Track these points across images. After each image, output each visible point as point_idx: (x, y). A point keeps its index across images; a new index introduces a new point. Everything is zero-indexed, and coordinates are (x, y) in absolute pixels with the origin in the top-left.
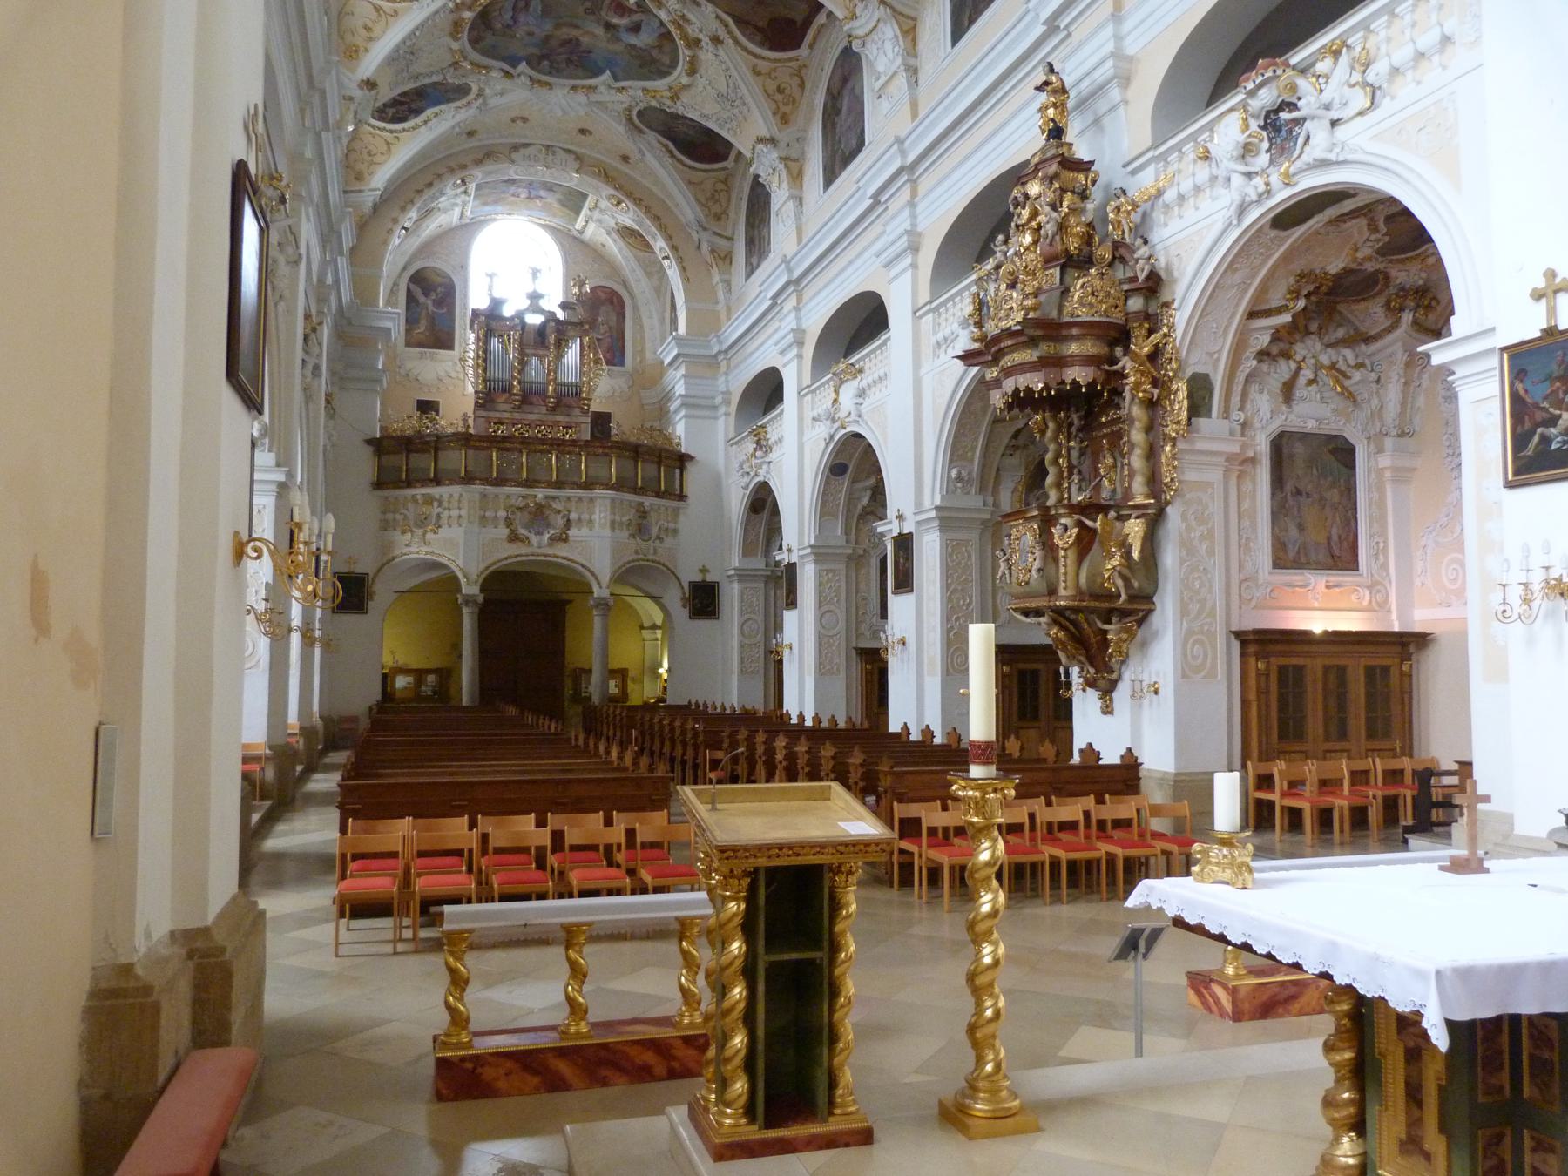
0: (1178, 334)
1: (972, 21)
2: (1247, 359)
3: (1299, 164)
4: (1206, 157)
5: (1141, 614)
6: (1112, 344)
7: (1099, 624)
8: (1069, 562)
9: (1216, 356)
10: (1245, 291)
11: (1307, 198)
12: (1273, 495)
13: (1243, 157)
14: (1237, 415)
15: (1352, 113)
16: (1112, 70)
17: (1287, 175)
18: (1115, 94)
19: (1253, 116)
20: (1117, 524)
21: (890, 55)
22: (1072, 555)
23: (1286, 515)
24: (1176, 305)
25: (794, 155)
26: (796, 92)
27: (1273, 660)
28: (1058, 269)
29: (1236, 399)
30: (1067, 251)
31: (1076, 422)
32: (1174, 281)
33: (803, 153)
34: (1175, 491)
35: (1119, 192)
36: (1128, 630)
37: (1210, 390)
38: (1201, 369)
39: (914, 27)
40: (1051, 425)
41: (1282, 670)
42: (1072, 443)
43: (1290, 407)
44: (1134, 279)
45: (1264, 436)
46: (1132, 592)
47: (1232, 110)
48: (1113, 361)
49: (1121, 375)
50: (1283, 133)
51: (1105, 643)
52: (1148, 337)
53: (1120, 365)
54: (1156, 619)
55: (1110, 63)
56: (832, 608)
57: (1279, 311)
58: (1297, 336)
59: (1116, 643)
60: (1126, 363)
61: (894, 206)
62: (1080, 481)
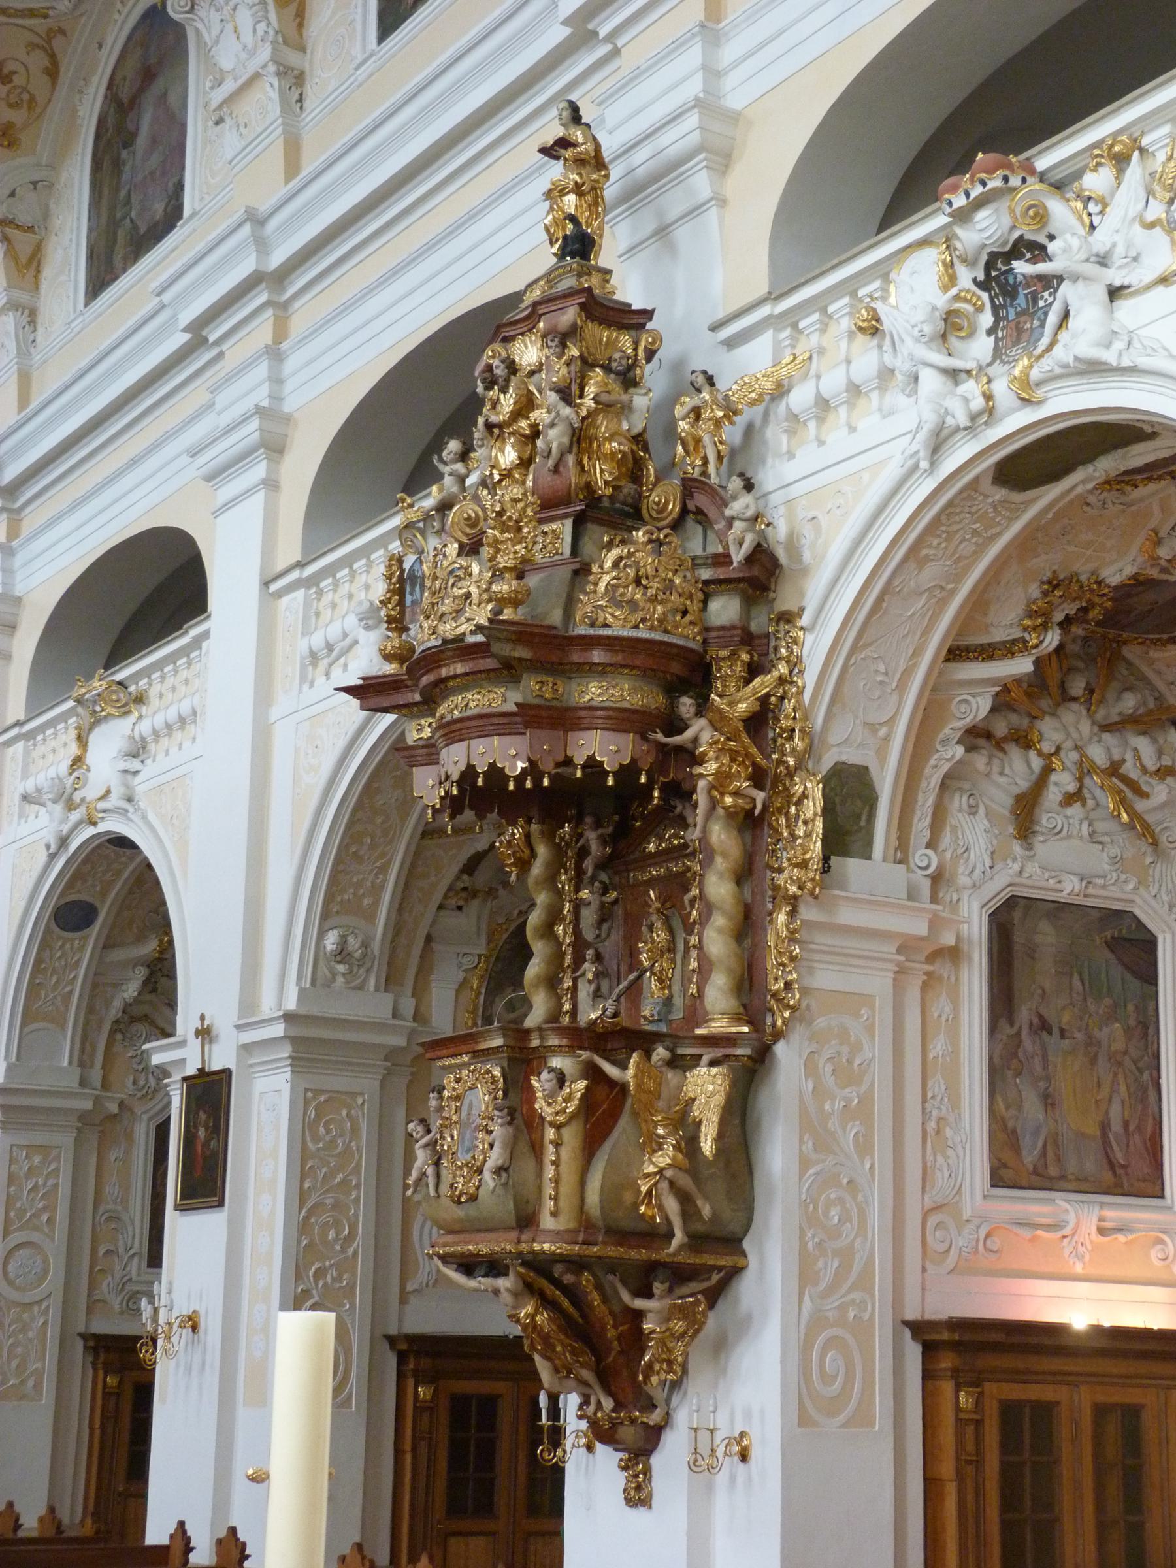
0: (809, 679)
2: (945, 742)
3: (1047, 364)
4: (873, 328)
5: (715, 1277)
6: (673, 690)
7: (626, 1297)
8: (565, 1153)
9: (883, 732)
10: (943, 603)
12: (993, 1028)
13: (944, 337)
14: (921, 856)
15: (1150, 276)
16: (695, 137)
17: (1025, 382)
18: (701, 183)
19: (964, 260)
20: (671, 1076)
21: (248, 38)
23: (1018, 1074)
24: (804, 621)
25: (24, 218)
26: (39, 85)
27: (989, 1387)
28: (569, 524)
29: (921, 825)
30: (589, 488)
31: (594, 847)
32: (804, 571)
33: (46, 215)
34: (794, 1009)
35: (701, 380)
36: (686, 1313)
37: (870, 800)
38: (852, 756)
40: (542, 850)
41: (1010, 1412)
42: (585, 894)
43: (1030, 847)
44: (723, 559)
45: (976, 906)
46: (699, 1227)
47: (924, 242)
48: (675, 725)
49: (690, 756)
50: (1021, 300)
51: (636, 1340)
52: (748, 681)
53: (689, 734)
54: (746, 1288)
56: (35, 1237)
57: (1009, 649)
58: (1045, 703)
59: (662, 1342)
60: (700, 732)
61: (237, 352)
62: (597, 975)
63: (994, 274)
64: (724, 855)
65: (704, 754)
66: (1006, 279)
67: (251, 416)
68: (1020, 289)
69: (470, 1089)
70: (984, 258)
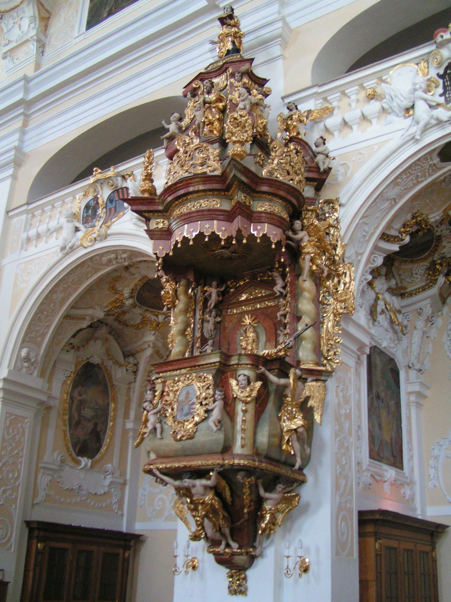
1: (110, 13)
9: (359, 258)
16: (280, 30)
18: (276, 50)
22: (251, 408)
31: (214, 297)
39: (49, 18)
40: (182, 297)
55: (280, 24)
64: (309, 292)
67: (12, 149)
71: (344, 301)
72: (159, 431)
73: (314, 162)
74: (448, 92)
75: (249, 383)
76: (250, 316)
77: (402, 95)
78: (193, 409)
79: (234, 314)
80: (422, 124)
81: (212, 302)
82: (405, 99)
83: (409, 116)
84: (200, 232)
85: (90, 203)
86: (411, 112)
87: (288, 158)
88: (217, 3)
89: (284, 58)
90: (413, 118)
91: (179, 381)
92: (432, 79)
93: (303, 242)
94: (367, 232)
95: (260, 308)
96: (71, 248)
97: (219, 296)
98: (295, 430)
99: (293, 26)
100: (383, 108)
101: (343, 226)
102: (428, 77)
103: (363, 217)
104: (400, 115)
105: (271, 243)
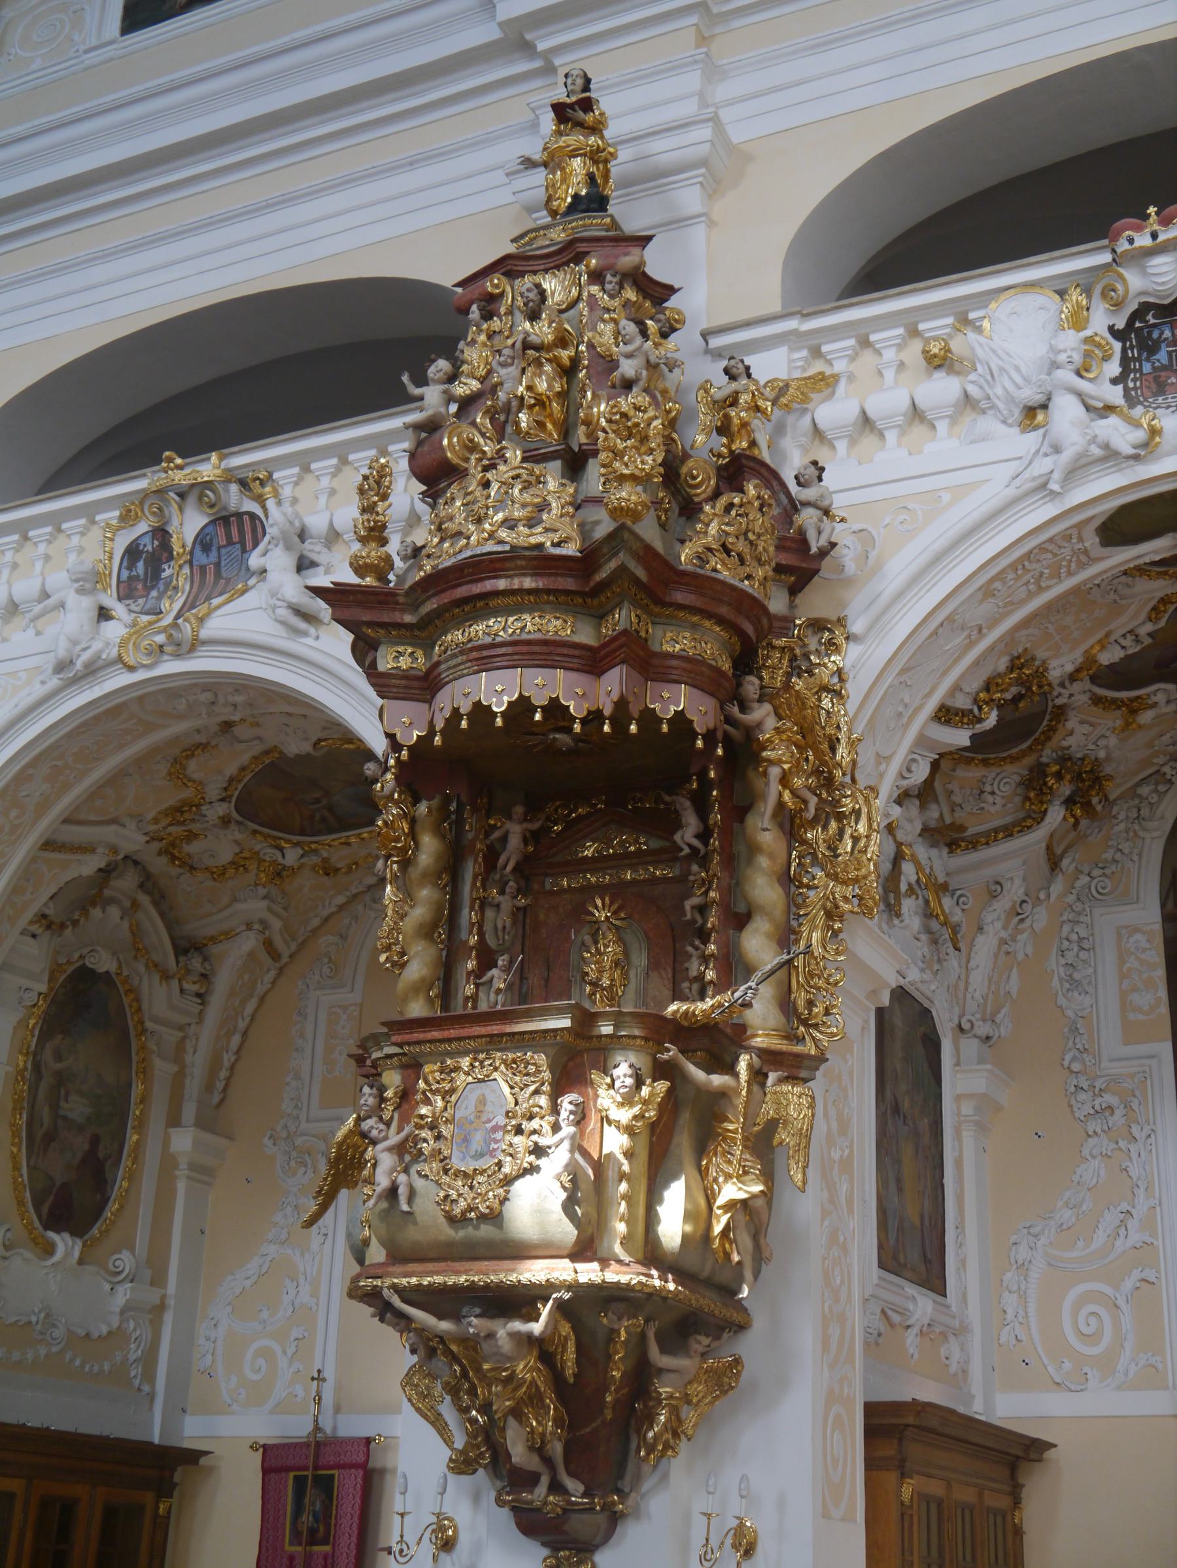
9: (883, 767)
11: (1160, 496)
31: (514, 842)
59: (675, 1411)
63: (1138, 325)
64: (771, 856)
65: (769, 740)
66: (1150, 333)
68: (1163, 345)
69: (480, 1081)
70: (1134, 306)
71: (856, 881)
72: (402, 1191)
73: (791, 523)
74: (1132, 376)
75: (639, 1083)
76: (607, 900)
77: (1017, 369)
78: (496, 1141)
79: (563, 891)
80: (1066, 456)
81: (510, 858)
82: (1027, 380)
83: (1036, 428)
84: (521, 695)
85: (142, 542)
86: (1040, 417)
87: (743, 520)
88: (528, 37)
89: (711, 224)
90: (1044, 436)
91: (457, 1069)
92: (1097, 339)
93: (762, 732)
94: (906, 706)
95: (634, 882)
96: (87, 665)
97: (525, 841)
98: (744, 1202)
99: (738, 135)
100: (966, 395)
101: (855, 690)
102: (1088, 333)
103: (904, 670)
104: (1010, 421)
105: (695, 735)
